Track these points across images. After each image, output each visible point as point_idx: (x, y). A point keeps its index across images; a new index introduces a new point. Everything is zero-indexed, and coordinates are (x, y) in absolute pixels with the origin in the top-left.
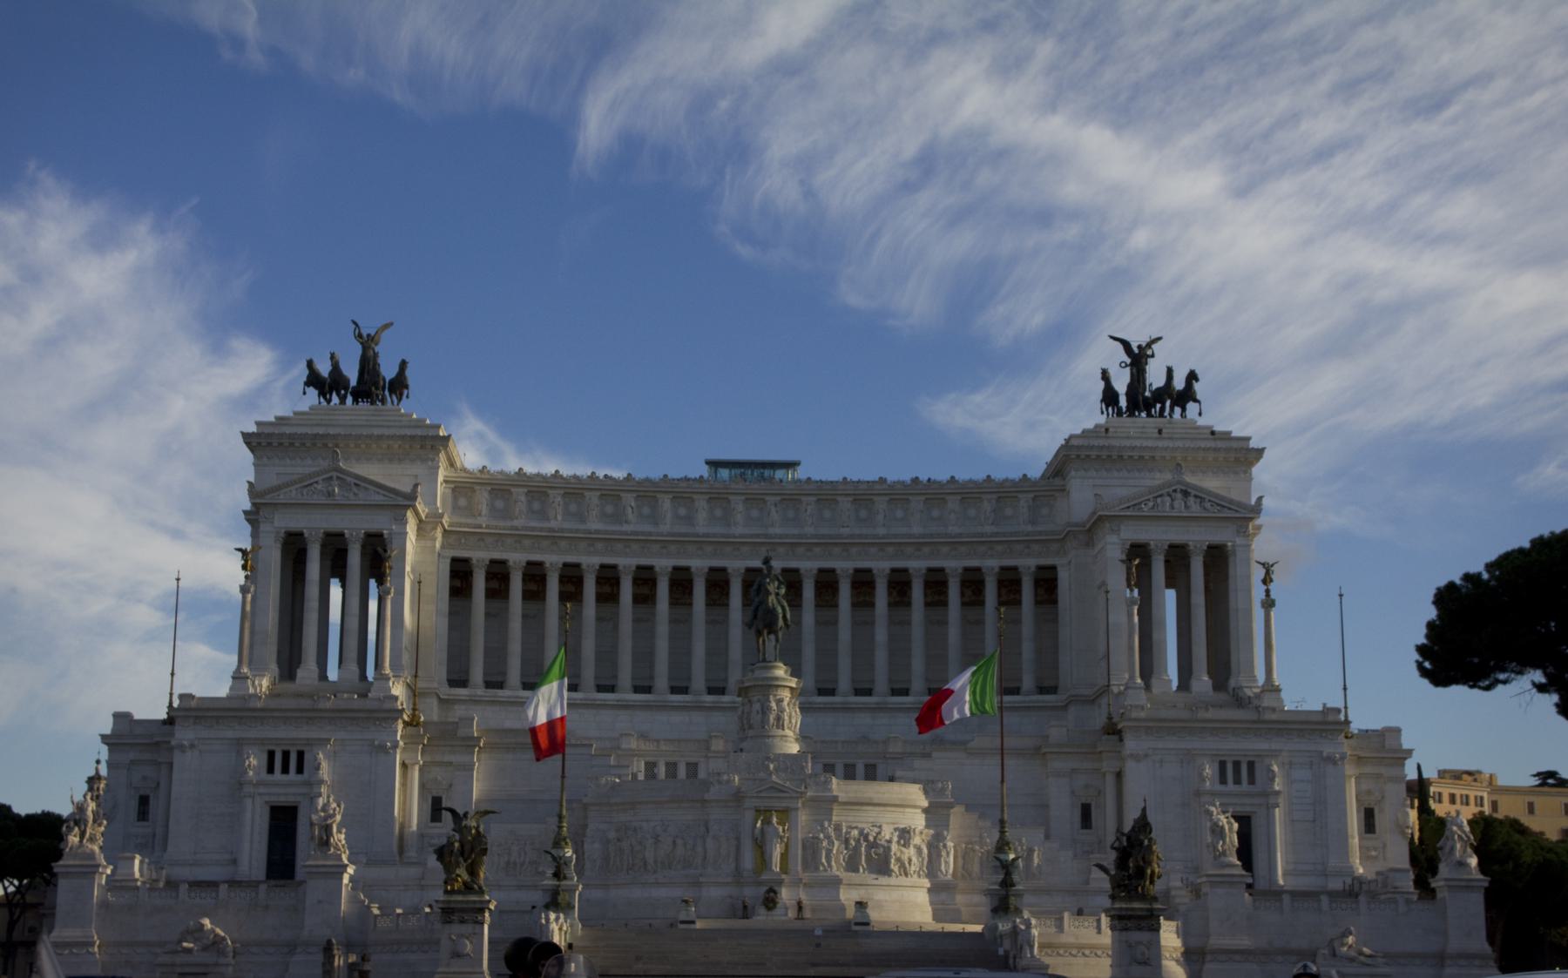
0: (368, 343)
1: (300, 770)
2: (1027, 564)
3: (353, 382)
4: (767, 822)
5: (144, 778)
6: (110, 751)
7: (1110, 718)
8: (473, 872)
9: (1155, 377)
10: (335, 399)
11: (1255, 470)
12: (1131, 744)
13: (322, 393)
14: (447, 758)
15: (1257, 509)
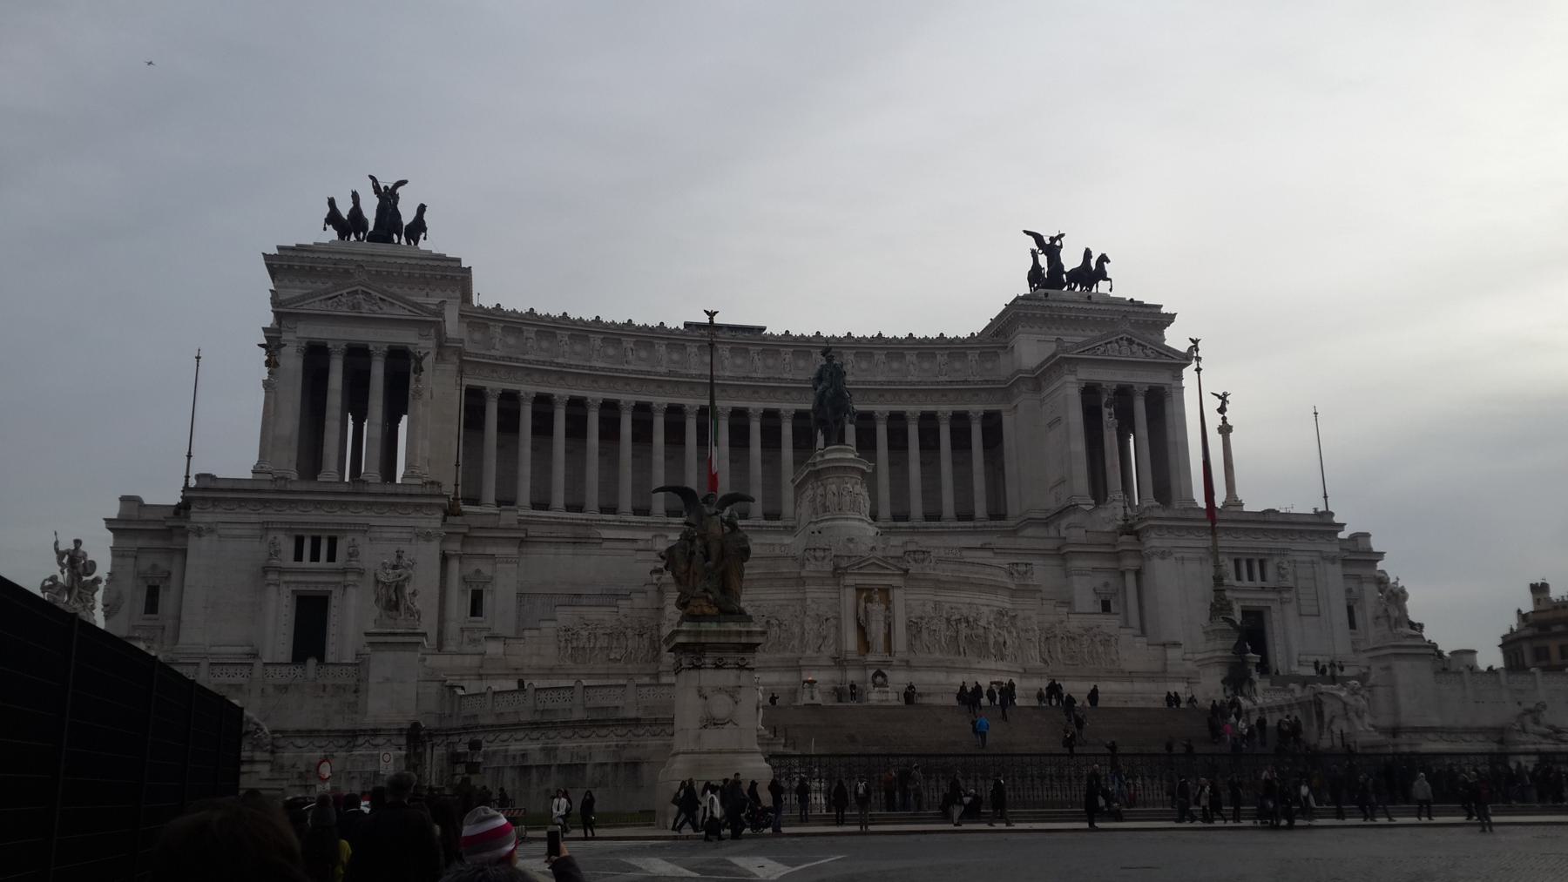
0: (388, 198)
1: (331, 557)
2: (976, 408)
3: (371, 228)
4: (869, 600)
5: (154, 566)
6: (115, 537)
7: (1126, 520)
8: (725, 589)
9: (1071, 260)
10: (353, 238)
11: (1167, 332)
12: (1154, 541)
13: (341, 236)
14: (489, 550)
15: (1191, 354)
